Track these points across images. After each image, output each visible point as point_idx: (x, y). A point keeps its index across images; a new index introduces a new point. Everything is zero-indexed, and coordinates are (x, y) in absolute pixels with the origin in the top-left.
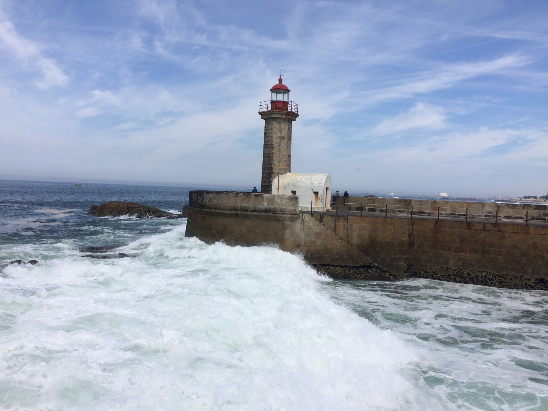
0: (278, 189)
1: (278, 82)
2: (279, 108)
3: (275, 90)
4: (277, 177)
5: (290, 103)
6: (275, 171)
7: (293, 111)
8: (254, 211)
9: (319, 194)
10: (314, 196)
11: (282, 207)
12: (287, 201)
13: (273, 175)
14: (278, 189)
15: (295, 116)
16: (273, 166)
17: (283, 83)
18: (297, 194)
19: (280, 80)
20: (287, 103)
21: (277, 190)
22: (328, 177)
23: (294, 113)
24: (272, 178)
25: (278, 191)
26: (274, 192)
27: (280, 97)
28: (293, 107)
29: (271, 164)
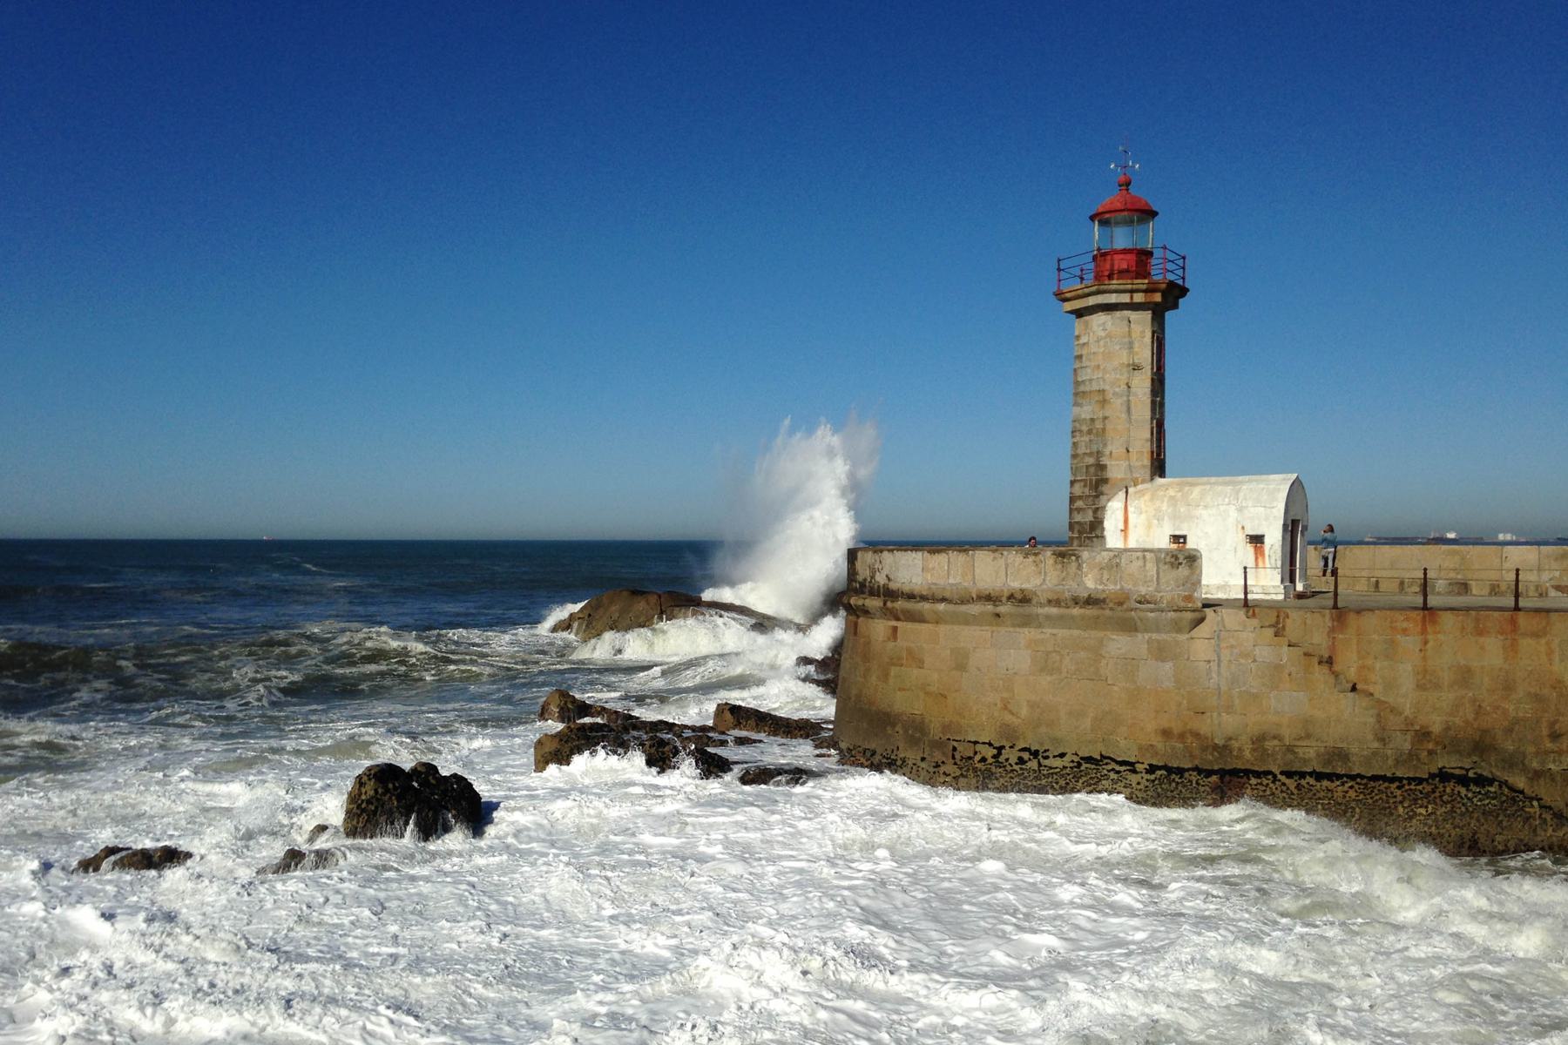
0: (1125, 530)
2: (1123, 273)
4: (1122, 495)
5: (1158, 253)
6: (1116, 471)
7: (1171, 277)
9: (1267, 540)
10: (1250, 549)
11: (1143, 590)
12: (1163, 567)
13: (1105, 488)
14: (1125, 530)
15: (1174, 293)
16: (1105, 461)
18: (1190, 545)
20: (1144, 255)
21: (1120, 536)
22: (1296, 490)
23: (1172, 284)
24: (1103, 498)
25: (1126, 537)
26: (1113, 539)
27: (1122, 238)
28: (1170, 266)
29: (1099, 454)
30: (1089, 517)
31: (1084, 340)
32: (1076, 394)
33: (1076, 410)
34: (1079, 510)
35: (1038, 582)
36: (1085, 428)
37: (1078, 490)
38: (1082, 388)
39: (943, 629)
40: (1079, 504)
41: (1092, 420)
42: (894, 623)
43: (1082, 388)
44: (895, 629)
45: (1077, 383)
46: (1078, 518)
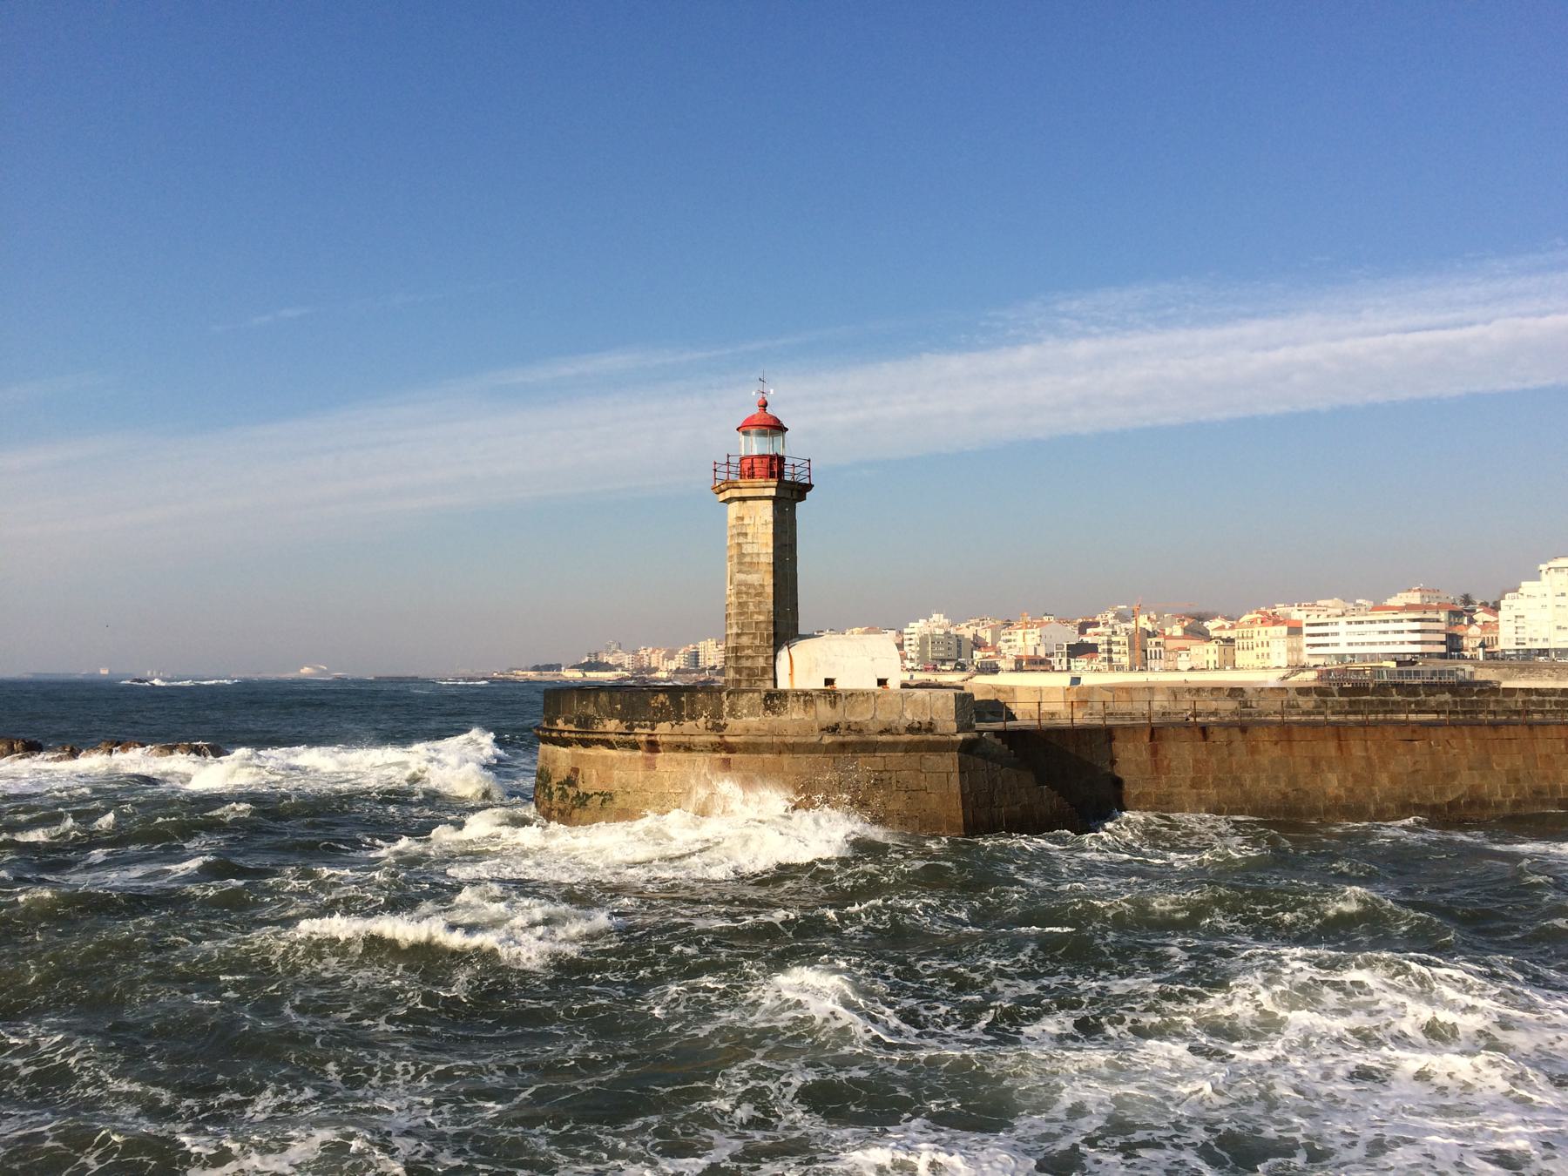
1: (755, 410)
8: (881, 733)
26: (783, 684)
30: (761, 662)
31: (746, 521)
32: (740, 563)
33: (742, 577)
34: (748, 657)
35: (869, 716)
36: (752, 591)
37: (745, 640)
38: (748, 559)
40: (749, 652)
41: (762, 586)
42: (724, 755)
43: (748, 559)
44: (726, 762)
45: (742, 555)
46: (748, 663)
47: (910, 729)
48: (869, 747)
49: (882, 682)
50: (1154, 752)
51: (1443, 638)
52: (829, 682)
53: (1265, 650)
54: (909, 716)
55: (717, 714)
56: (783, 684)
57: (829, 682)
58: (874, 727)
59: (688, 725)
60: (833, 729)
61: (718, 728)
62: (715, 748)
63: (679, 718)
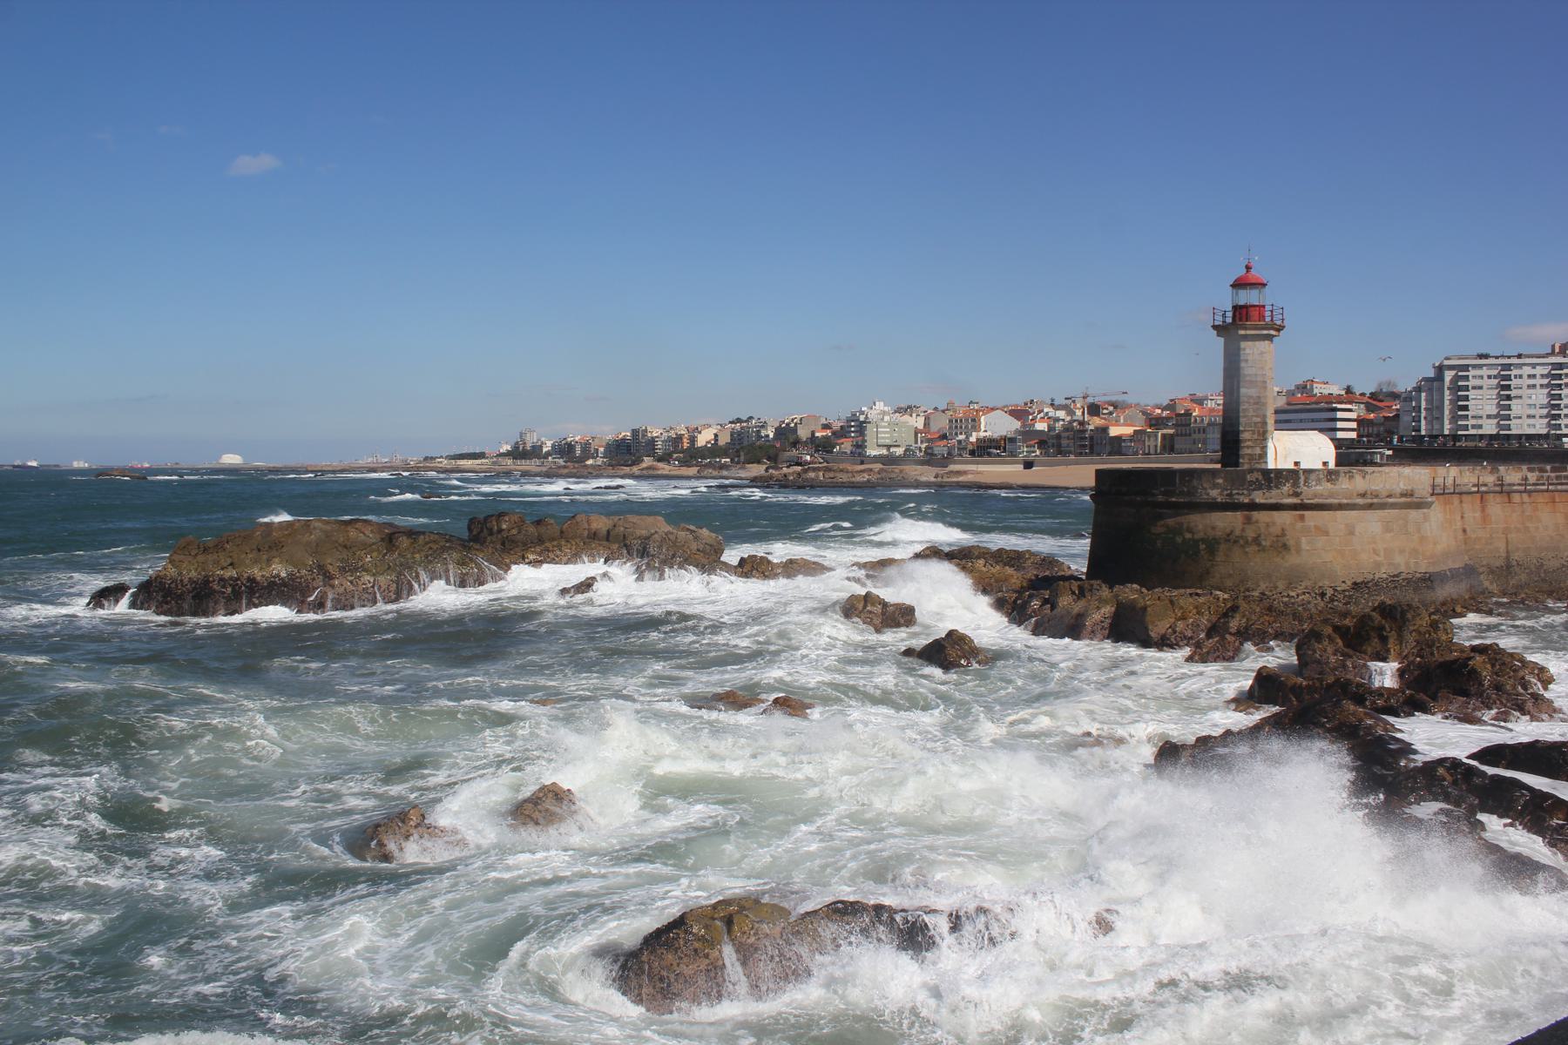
3: (1239, 284)
5: (1268, 308)
8: (1390, 496)
17: (1253, 271)
19: (1248, 268)
27: (1248, 297)
30: (1258, 451)
39: (1339, 513)
47: (1402, 495)
48: (1383, 506)
49: (1325, 464)
50: (1483, 509)
51: (1354, 425)
52: (1296, 464)
53: (1202, 436)
54: (1402, 486)
55: (1296, 484)
56: (1271, 466)
57: (1296, 464)
58: (1385, 494)
59: (1274, 492)
60: (1363, 495)
61: (1296, 495)
62: (1294, 507)
63: (1269, 488)
